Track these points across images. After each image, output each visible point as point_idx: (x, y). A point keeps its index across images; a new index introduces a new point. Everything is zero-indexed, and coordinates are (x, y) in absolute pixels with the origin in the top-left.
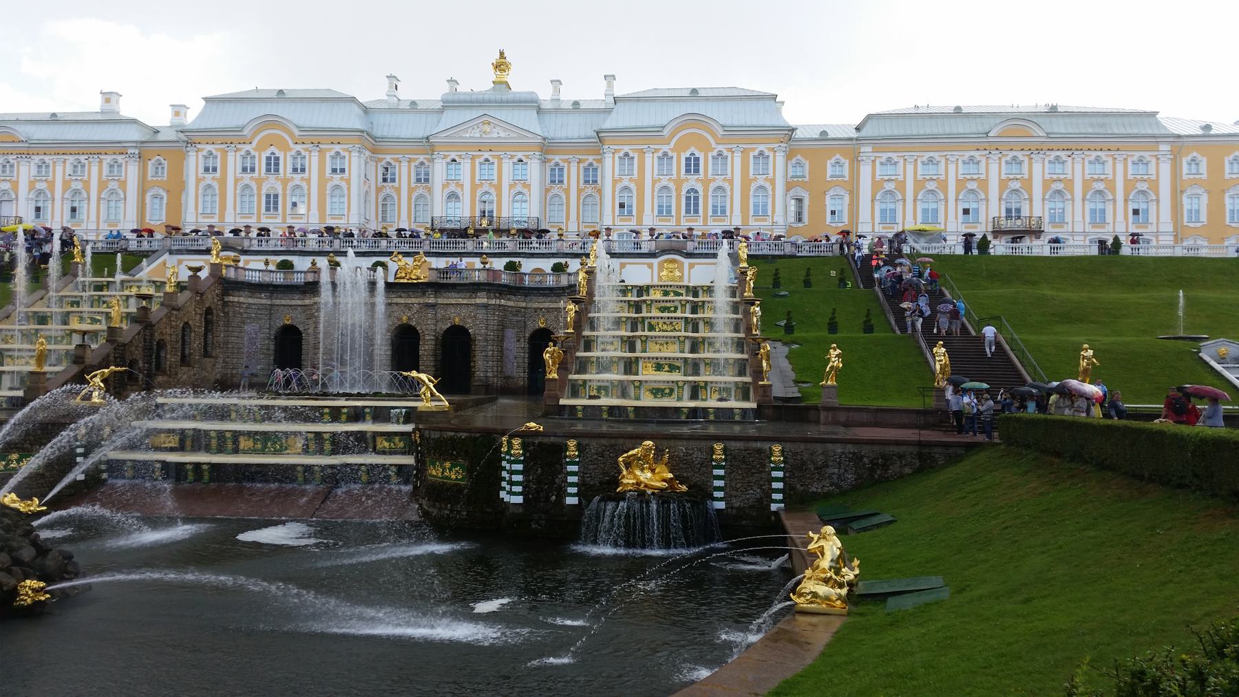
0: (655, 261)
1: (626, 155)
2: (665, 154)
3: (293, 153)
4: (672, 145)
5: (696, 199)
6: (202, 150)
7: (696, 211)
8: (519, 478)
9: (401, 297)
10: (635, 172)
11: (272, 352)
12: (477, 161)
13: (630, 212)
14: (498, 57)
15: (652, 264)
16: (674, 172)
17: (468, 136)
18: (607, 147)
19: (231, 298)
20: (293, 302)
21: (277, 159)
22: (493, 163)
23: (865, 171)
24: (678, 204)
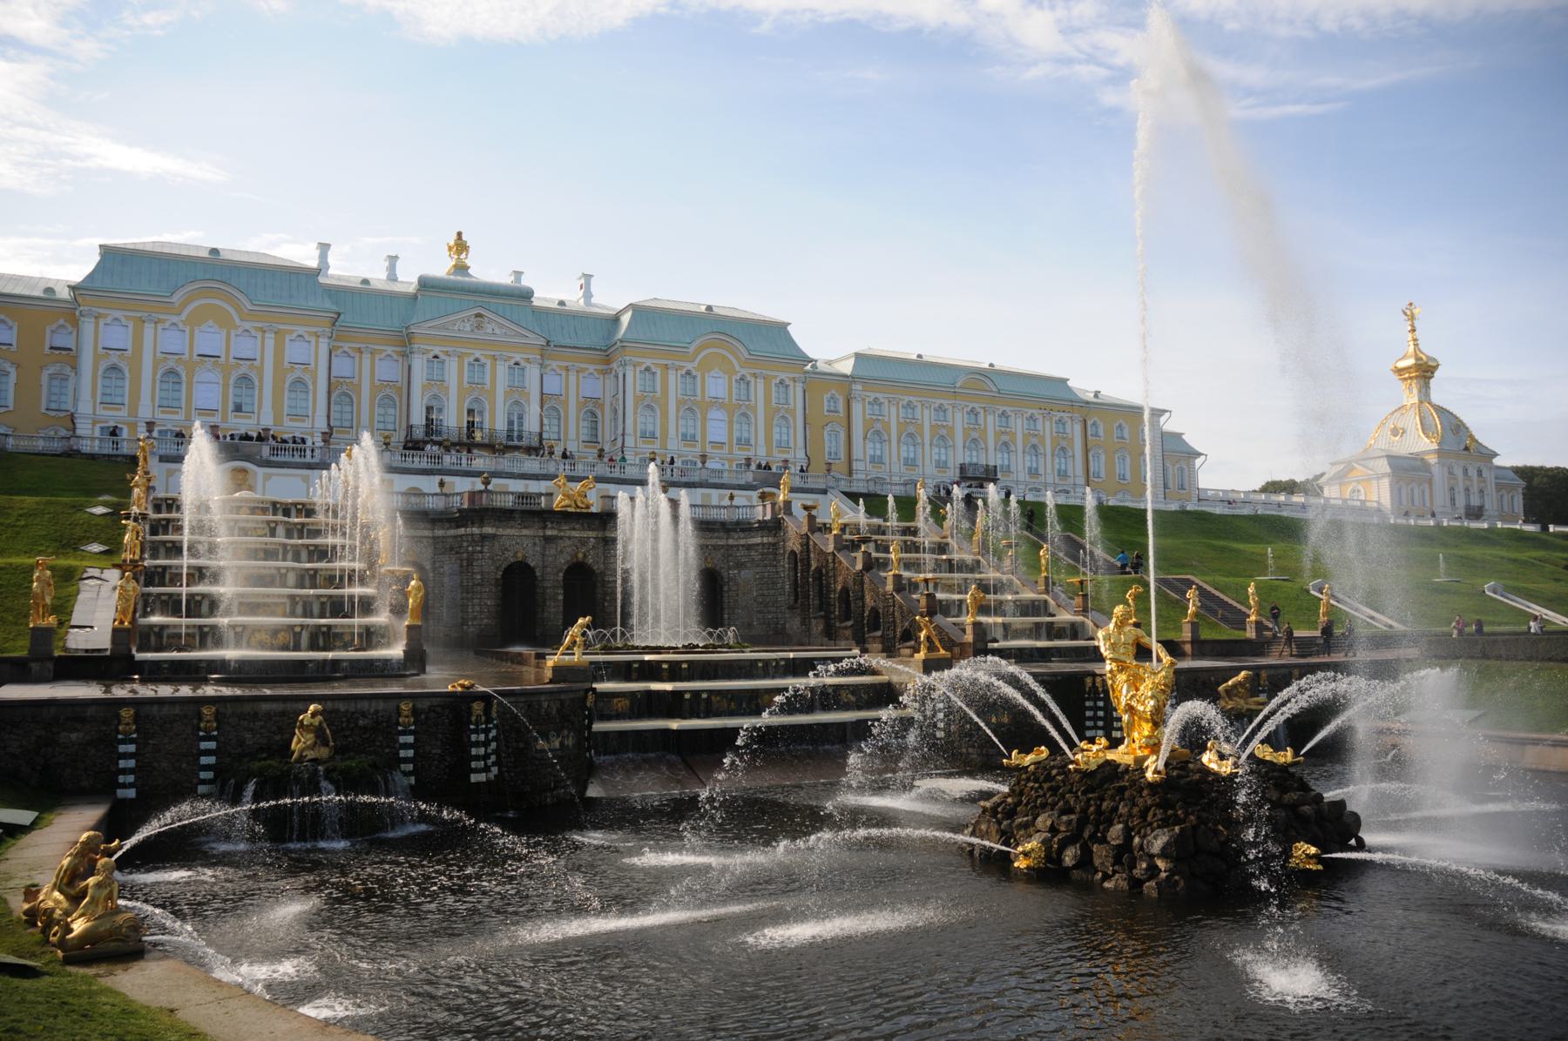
1: (647, 369)
2: (688, 373)
3: (240, 331)
4: (695, 364)
6: (105, 316)
9: (574, 529)
10: (658, 388)
14: (455, 237)
15: (751, 497)
17: (456, 328)
18: (628, 358)
22: (483, 365)
23: (857, 408)
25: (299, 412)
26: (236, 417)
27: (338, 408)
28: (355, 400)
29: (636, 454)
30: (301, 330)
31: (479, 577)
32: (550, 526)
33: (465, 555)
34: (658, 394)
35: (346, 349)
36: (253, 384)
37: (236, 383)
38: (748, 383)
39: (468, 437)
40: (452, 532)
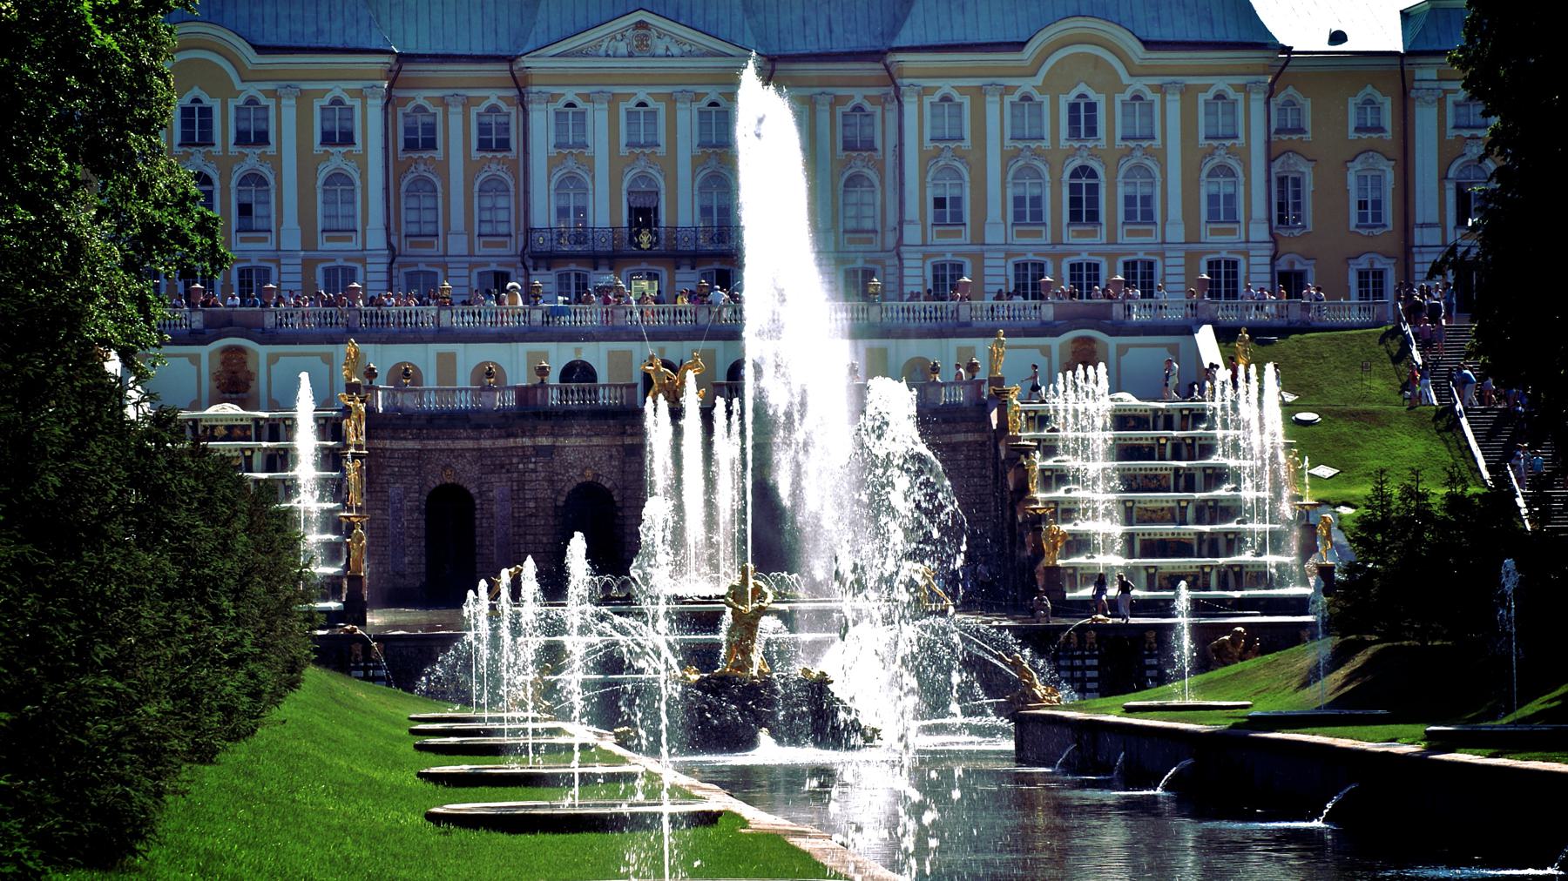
0: (1055, 343)
3: (241, 101)
4: (1039, 80)
5: (1094, 189)
7: (1093, 217)
8: (1095, 674)
10: (967, 134)
11: (422, 533)
12: (623, 107)
13: (958, 219)
15: (1049, 347)
16: (1047, 135)
19: (379, 444)
20: (459, 444)
21: (207, 112)
22: (654, 113)
23: (1425, 120)
24: (1056, 202)
25: (341, 224)
26: (243, 240)
27: (413, 203)
28: (439, 189)
29: (926, 257)
30: (337, 89)
31: (532, 504)
32: (629, 432)
33: (515, 475)
34: (967, 143)
35: (421, 101)
36: (266, 183)
37: (240, 184)
38: (1151, 104)
39: (631, 241)
40: (501, 443)
